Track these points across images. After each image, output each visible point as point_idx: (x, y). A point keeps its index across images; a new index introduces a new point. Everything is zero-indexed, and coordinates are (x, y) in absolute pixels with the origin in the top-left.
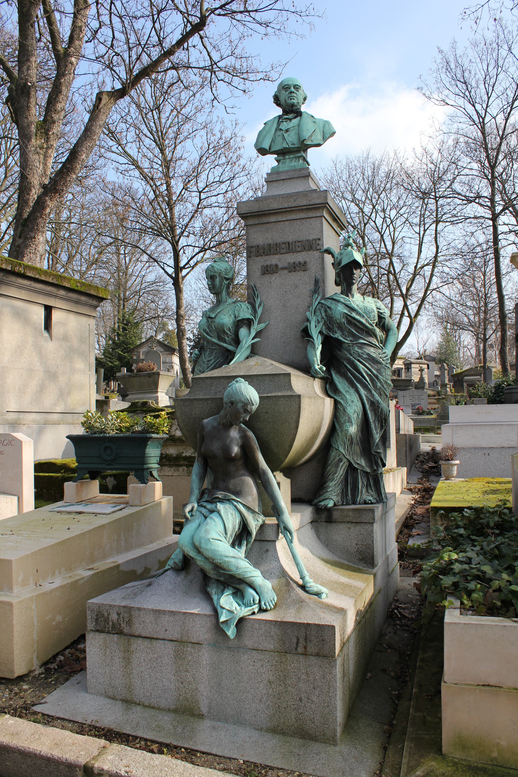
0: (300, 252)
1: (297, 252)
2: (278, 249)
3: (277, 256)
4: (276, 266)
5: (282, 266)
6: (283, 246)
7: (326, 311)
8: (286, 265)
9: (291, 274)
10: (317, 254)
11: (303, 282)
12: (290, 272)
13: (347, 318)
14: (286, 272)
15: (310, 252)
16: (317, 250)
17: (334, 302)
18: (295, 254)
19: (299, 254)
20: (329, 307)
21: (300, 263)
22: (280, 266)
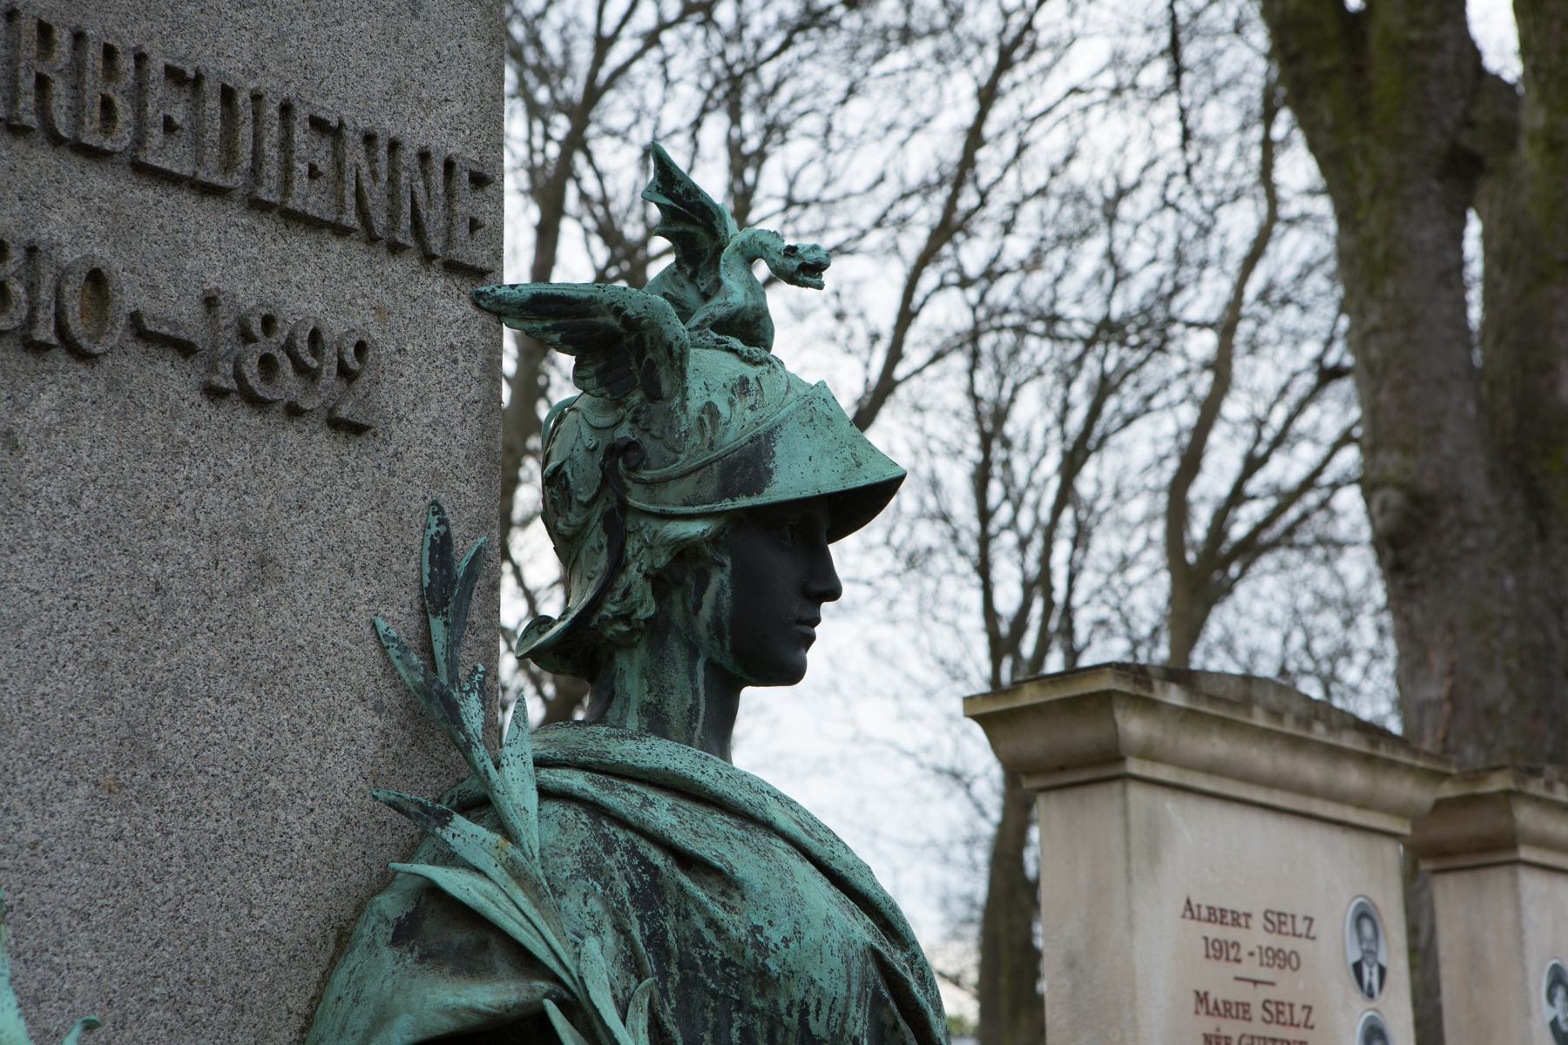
0: (313, 224)
1: (293, 218)
2: (124, 112)
3: (98, 181)
4: (97, 279)
5: (145, 303)
6: (164, 101)
7: (651, 893)
8: (184, 314)
9: (218, 416)
10: (451, 304)
11: (319, 538)
12: (214, 394)
13: (877, 1001)
14: (175, 380)
15: (398, 269)
16: (454, 268)
17: (718, 822)
18: (267, 226)
19: (302, 243)
20: (687, 861)
21: (315, 337)
22: (129, 296)
